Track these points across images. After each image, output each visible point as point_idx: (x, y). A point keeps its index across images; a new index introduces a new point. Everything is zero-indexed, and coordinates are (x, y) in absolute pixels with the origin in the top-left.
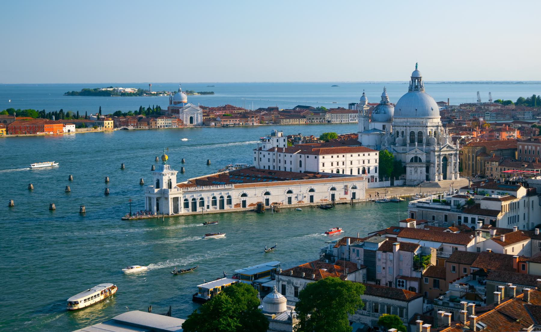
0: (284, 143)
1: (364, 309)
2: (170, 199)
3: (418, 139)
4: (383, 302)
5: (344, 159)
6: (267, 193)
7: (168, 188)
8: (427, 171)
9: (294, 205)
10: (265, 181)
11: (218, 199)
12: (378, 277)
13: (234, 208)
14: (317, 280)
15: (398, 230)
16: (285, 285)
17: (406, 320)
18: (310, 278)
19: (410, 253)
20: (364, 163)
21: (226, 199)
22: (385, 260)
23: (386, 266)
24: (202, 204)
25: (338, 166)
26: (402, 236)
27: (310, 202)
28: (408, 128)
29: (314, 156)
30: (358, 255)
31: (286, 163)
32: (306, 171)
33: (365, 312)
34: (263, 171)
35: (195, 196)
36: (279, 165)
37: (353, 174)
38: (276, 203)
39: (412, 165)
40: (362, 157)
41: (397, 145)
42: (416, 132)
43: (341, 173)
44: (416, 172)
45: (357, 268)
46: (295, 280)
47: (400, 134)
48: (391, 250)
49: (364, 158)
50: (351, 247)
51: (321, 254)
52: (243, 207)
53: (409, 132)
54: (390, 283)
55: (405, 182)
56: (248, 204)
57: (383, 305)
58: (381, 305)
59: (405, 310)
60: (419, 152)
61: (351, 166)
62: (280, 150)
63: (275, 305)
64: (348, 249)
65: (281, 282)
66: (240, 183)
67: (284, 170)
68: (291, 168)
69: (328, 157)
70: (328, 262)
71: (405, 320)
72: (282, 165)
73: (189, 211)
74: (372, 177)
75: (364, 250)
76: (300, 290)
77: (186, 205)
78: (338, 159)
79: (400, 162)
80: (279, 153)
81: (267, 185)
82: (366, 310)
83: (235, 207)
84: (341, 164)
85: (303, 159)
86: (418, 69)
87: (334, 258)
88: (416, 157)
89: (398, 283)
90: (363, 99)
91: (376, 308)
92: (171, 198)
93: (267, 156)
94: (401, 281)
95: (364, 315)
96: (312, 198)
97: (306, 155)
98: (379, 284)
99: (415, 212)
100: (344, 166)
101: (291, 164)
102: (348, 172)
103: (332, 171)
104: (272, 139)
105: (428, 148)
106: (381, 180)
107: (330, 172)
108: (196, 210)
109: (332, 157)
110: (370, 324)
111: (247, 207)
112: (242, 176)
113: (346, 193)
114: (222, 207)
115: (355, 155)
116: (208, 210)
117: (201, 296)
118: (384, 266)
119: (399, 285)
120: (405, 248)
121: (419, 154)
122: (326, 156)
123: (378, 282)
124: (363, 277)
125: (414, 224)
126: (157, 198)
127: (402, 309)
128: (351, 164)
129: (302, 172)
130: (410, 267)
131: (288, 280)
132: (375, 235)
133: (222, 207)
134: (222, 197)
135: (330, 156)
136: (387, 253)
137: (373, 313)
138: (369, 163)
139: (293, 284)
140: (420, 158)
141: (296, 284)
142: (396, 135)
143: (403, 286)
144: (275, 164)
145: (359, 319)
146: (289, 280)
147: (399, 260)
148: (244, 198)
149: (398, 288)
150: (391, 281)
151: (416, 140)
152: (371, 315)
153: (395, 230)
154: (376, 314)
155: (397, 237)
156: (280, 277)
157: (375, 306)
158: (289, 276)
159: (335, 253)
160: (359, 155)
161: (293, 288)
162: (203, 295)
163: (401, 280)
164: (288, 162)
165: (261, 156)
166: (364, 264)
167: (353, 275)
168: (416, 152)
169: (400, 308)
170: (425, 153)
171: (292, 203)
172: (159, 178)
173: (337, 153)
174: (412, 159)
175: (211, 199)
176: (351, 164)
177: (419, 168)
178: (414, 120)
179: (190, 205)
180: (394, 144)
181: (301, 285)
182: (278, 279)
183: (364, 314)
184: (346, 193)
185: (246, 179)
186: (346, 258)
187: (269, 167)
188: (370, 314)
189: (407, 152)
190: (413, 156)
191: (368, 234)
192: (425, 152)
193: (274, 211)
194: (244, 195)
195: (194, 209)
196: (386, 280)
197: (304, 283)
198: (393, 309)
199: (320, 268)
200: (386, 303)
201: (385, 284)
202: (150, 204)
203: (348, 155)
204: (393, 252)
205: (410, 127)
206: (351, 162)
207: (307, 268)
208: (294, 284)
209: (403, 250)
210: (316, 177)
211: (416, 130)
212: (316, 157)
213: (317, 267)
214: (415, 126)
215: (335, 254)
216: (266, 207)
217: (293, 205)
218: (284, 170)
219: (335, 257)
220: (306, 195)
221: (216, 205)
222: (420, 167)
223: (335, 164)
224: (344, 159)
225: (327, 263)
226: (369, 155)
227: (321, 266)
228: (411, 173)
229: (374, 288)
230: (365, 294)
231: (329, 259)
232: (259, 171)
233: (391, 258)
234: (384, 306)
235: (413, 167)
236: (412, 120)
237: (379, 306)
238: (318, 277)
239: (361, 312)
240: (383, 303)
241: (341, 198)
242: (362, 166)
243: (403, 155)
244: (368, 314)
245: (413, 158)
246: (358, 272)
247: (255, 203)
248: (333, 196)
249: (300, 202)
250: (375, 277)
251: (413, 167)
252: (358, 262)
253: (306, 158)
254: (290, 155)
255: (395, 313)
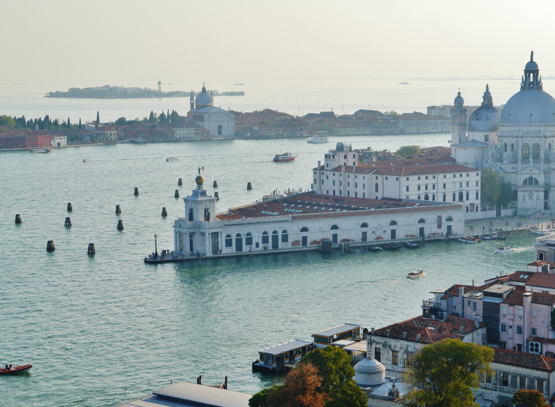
0: (354, 160)
1: (489, 381)
2: (207, 235)
3: (534, 154)
4: (514, 372)
5: (434, 181)
6: (335, 227)
7: (205, 220)
8: (546, 196)
9: (371, 242)
10: (331, 211)
11: (270, 235)
12: (504, 337)
13: (291, 247)
14: (423, 343)
15: (526, 277)
16: (380, 349)
17: (548, 396)
18: (415, 340)
19: (545, 307)
20: (461, 186)
21: (280, 234)
22: (512, 316)
23: (513, 324)
24: (249, 241)
25: (427, 191)
26: (532, 284)
27: (392, 238)
28: (520, 139)
29: (395, 177)
30: (475, 309)
31: (356, 187)
32: (384, 197)
33: (489, 385)
34: (327, 198)
35: (241, 232)
36: (348, 189)
37: (447, 201)
38: (348, 240)
39: (526, 189)
40: (458, 179)
41: (505, 162)
42: (531, 144)
43: (431, 199)
44: (531, 197)
45: (474, 326)
46: (393, 343)
47: (509, 147)
48: (521, 303)
49: (461, 179)
50: (465, 299)
51: (425, 308)
52: (303, 245)
53: (521, 144)
54: (520, 346)
55: (516, 212)
56: (309, 241)
57: (514, 376)
58: (512, 376)
59: (545, 383)
60: (534, 171)
61: (445, 190)
62: (349, 169)
63: (370, 375)
64: (461, 301)
65: (374, 345)
66: (298, 213)
67: (362, 197)
68: (364, 194)
69: (414, 179)
70: (435, 318)
71: (545, 396)
72: (351, 189)
73: (232, 250)
74: (472, 204)
75: (484, 302)
76: (400, 355)
77: (229, 243)
78: (426, 182)
79: (509, 185)
80: (347, 174)
81: (335, 216)
82: (491, 383)
83: (292, 245)
84: (430, 187)
85: (379, 181)
86: (534, 60)
87: (442, 313)
88: (531, 179)
89: (530, 347)
90: (459, 100)
91: (505, 379)
92: (209, 234)
93: (331, 178)
94: (534, 344)
95: (489, 389)
96: (393, 232)
97: (384, 176)
98: (505, 347)
99: (545, 252)
100: (435, 191)
101: (364, 188)
102: (440, 199)
103: (419, 198)
104: (338, 154)
105: (546, 166)
106: (483, 210)
107: (416, 199)
108: (241, 250)
109: (419, 178)
110: (497, 401)
111: (308, 245)
112: (300, 204)
113: (439, 226)
114: (275, 245)
115: (450, 176)
116: (258, 249)
117: (264, 364)
118: (511, 323)
119: (532, 349)
120: (540, 301)
121: (536, 174)
122: (411, 178)
123: (503, 345)
124: (483, 338)
125: (547, 268)
126: (190, 233)
127: (541, 381)
128: (444, 187)
129: (379, 198)
130: (547, 325)
131: (383, 342)
132: (496, 282)
133: (275, 245)
134: (275, 232)
135: (416, 177)
136: (516, 306)
137: (500, 387)
138: (468, 186)
139: (390, 347)
140: (536, 180)
141: (395, 347)
142: (503, 149)
143: (537, 350)
144: (342, 188)
145: (481, 395)
146: (385, 342)
147: (531, 315)
148: (304, 234)
149: (530, 352)
150: (521, 343)
151: (531, 155)
152: (498, 389)
153: (522, 276)
154: (505, 388)
155: (526, 285)
156: (373, 338)
157: (503, 377)
158: (386, 336)
159: (444, 307)
160: (454, 176)
161: (391, 352)
162: (266, 362)
163: (535, 343)
164: (360, 186)
165: (324, 177)
166: (483, 320)
167: (470, 335)
168: (531, 171)
169: (538, 381)
170: (543, 173)
171: (368, 240)
172: (193, 206)
173: (426, 173)
174: (525, 182)
175: (261, 235)
176: (444, 187)
177: (535, 193)
178: (528, 128)
179: (234, 242)
180: (501, 160)
181: (401, 348)
182: (370, 341)
183: (488, 387)
184: (439, 226)
185: (305, 208)
186: (459, 313)
187: (334, 191)
188: (496, 387)
189: (518, 172)
190: (527, 176)
191: (485, 281)
192: (544, 172)
193: (345, 251)
194: (305, 229)
195: (239, 247)
196: (513, 344)
197: (405, 347)
198: (528, 382)
199: (426, 326)
200: (519, 373)
201: (512, 347)
202: (181, 241)
203: (441, 176)
204: (523, 306)
205: (522, 137)
206: (444, 185)
207: (408, 327)
208: (392, 348)
209: (537, 303)
210: (399, 206)
211: (531, 142)
212: (397, 179)
213: (422, 325)
214: (530, 137)
215: (443, 307)
216: (335, 246)
217: (369, 242)
218: (362, 197)
219: (443, 312)
220: (386, 229)
221: (268, 242)
222: (537, 191)
223: (423, 188)
224: (434, 181)
225: (433, 320)
226: (468, 175)
227: (427, 323)
228: (524, 199)
229: (501, 353)
230: (496, 361)
231: (437, 315)
232: (321, 196)
233: (521, 313)
234: (516, 377)
235: (527, 191)
236: (525, 129)
237: (510, 377)
238: (425, 338)
239: (483, 385)
240: (515, 373)
241: (432, 233)
242: (459, 190)
243: (513, 175)
244: (494, 387)
245: (527, 178)
246: (477, 332)
247: (318, 240)
248: (422, 230)
249: (378, 238)
250: (498, 337)
251: (527, 191)
252: (476, 318)
253: (385, 181)
254: (362, 176)
255: (531, 386)
